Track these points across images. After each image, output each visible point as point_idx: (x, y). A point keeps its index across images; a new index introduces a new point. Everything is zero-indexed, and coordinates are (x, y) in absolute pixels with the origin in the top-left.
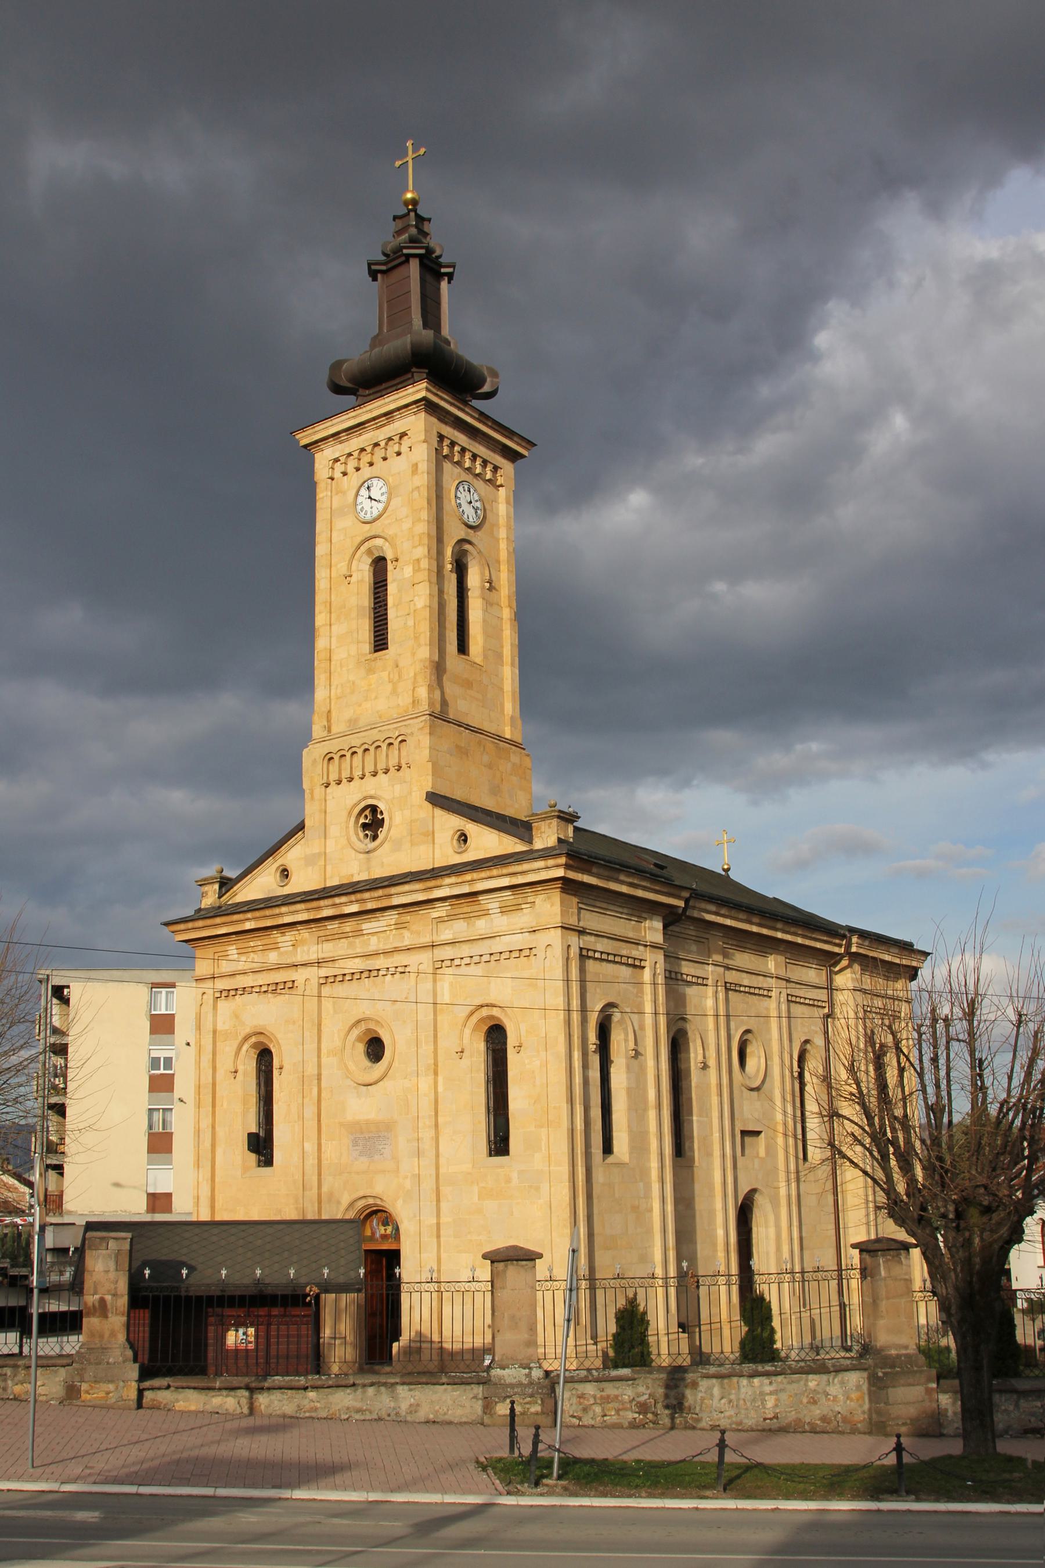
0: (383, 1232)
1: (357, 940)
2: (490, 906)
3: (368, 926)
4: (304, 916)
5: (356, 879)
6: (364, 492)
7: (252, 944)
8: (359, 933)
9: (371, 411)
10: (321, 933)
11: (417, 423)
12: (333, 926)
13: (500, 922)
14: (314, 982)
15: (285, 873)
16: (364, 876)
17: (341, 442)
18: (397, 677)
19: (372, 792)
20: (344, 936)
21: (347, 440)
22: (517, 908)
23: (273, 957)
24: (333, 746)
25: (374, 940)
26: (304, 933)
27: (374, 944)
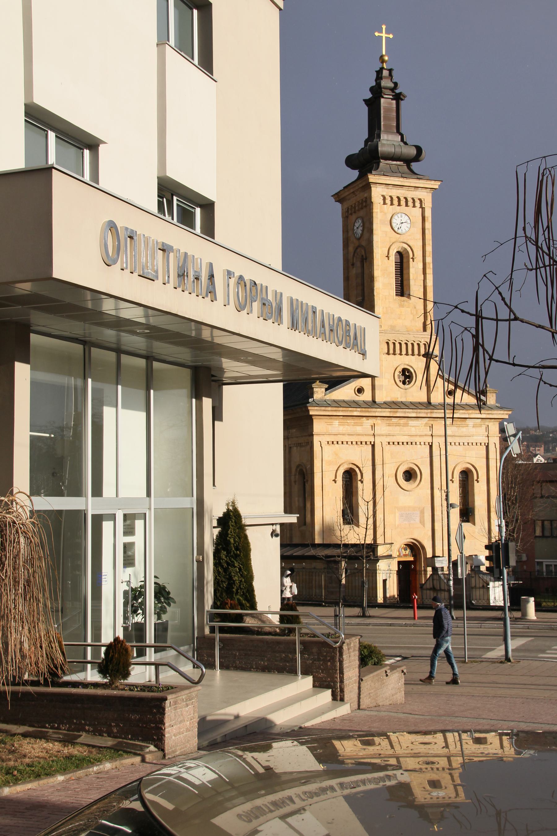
0: (404, 553)
1: (405, 428)
2: (469, 423)
3: (412, 422)
4: (388, 415)
5: (400, 400)
6: (409, 221)
7: (348, 421)
8: (406, 425)
9: (410, 182)
10: (388, 422)
11: (427, 198)
12: (394, 420)
13: (472, 430)
14: (385, 444)
15: (360, 390)
16: (403, 400)
17: (387, 188)
18: (415, 313)
19: (407, 363)
20: (398, 425)
21: (391, 189)
22: (480, 426)
23: (359, 429)
24: (392, 338)
25: (413, 429)
26: (378, 421)
27: (413, 431)
